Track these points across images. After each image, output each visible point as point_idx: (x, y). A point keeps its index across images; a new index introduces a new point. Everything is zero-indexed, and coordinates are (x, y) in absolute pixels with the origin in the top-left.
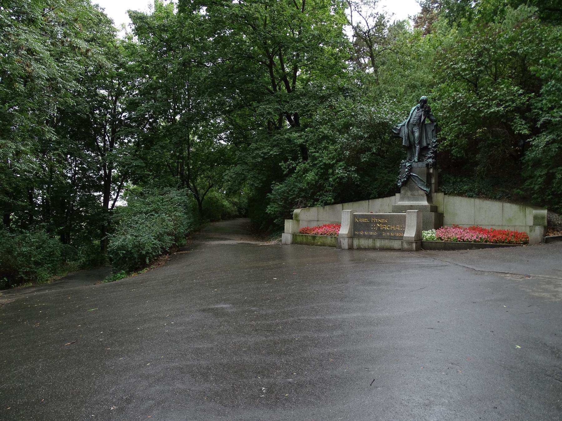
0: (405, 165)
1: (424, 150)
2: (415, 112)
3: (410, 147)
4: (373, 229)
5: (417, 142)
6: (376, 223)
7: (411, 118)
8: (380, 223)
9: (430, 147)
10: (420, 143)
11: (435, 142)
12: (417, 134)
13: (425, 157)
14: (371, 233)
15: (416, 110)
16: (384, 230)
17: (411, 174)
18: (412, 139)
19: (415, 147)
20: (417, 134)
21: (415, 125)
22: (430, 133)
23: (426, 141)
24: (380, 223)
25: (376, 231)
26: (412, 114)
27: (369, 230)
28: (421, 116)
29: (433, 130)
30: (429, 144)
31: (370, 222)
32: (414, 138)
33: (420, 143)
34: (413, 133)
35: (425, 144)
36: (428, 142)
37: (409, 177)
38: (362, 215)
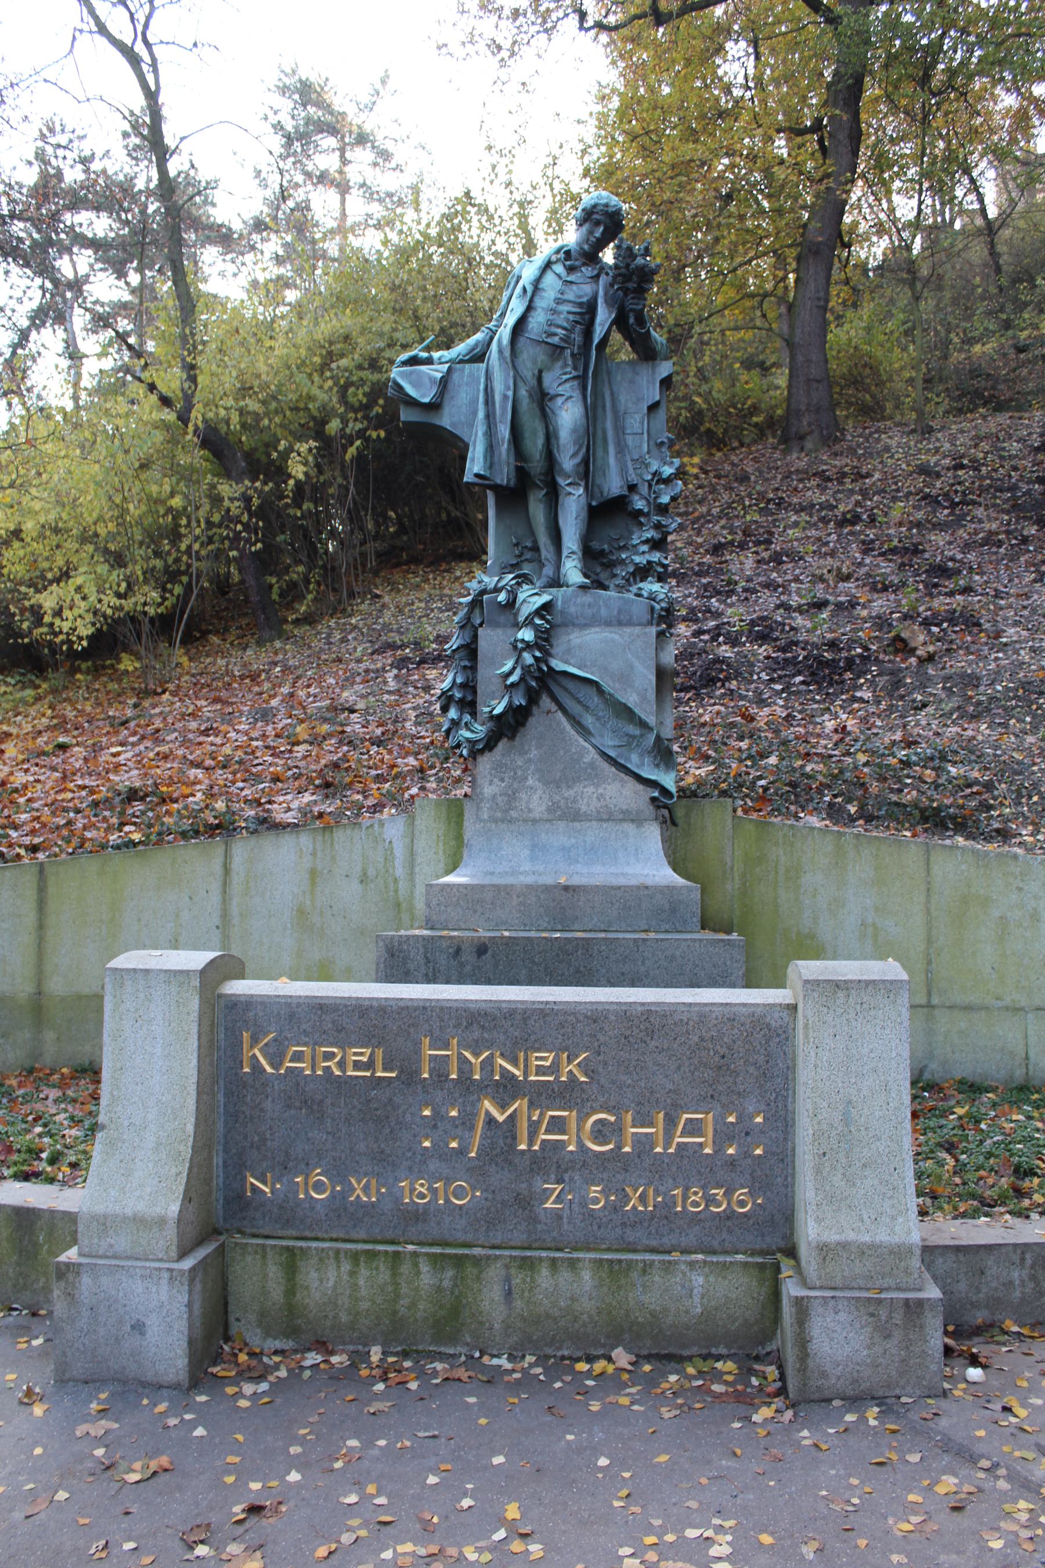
0: (511, 604)
1: (607, 512)
2: (549, 279)
3: (528, 483)
4: (440, 1152)
5: (568, 462)
6: (467, 1088)
7: (529, 308)
8: (507, 1089)
9: (639, 504)
10: (586, 471)
11: (667, 481)
12: (568, 415)
13: (611, 565)
14: (417, 1191)
15: (559, 268)
16: (550, 1162)
17: (558, 665)
18: (535, 445)
19: (553, 497)
20: (568, 415)
21: (556, 351)
22: (636, 421)
23: (623, 470)
24: (507, 1089)
25: (477, 1172)
26: (537, 283)
27: (384, 1163)
28: (590, 309)
29: (653, 408)
30: (632, 488)
31: (409, 1076)
32: (550, 436)
33: (586, 471)
34: (542, 399)
35: (613, 485)
36: (633, 478)
37: (542, 683)
38: (322, 1007)
